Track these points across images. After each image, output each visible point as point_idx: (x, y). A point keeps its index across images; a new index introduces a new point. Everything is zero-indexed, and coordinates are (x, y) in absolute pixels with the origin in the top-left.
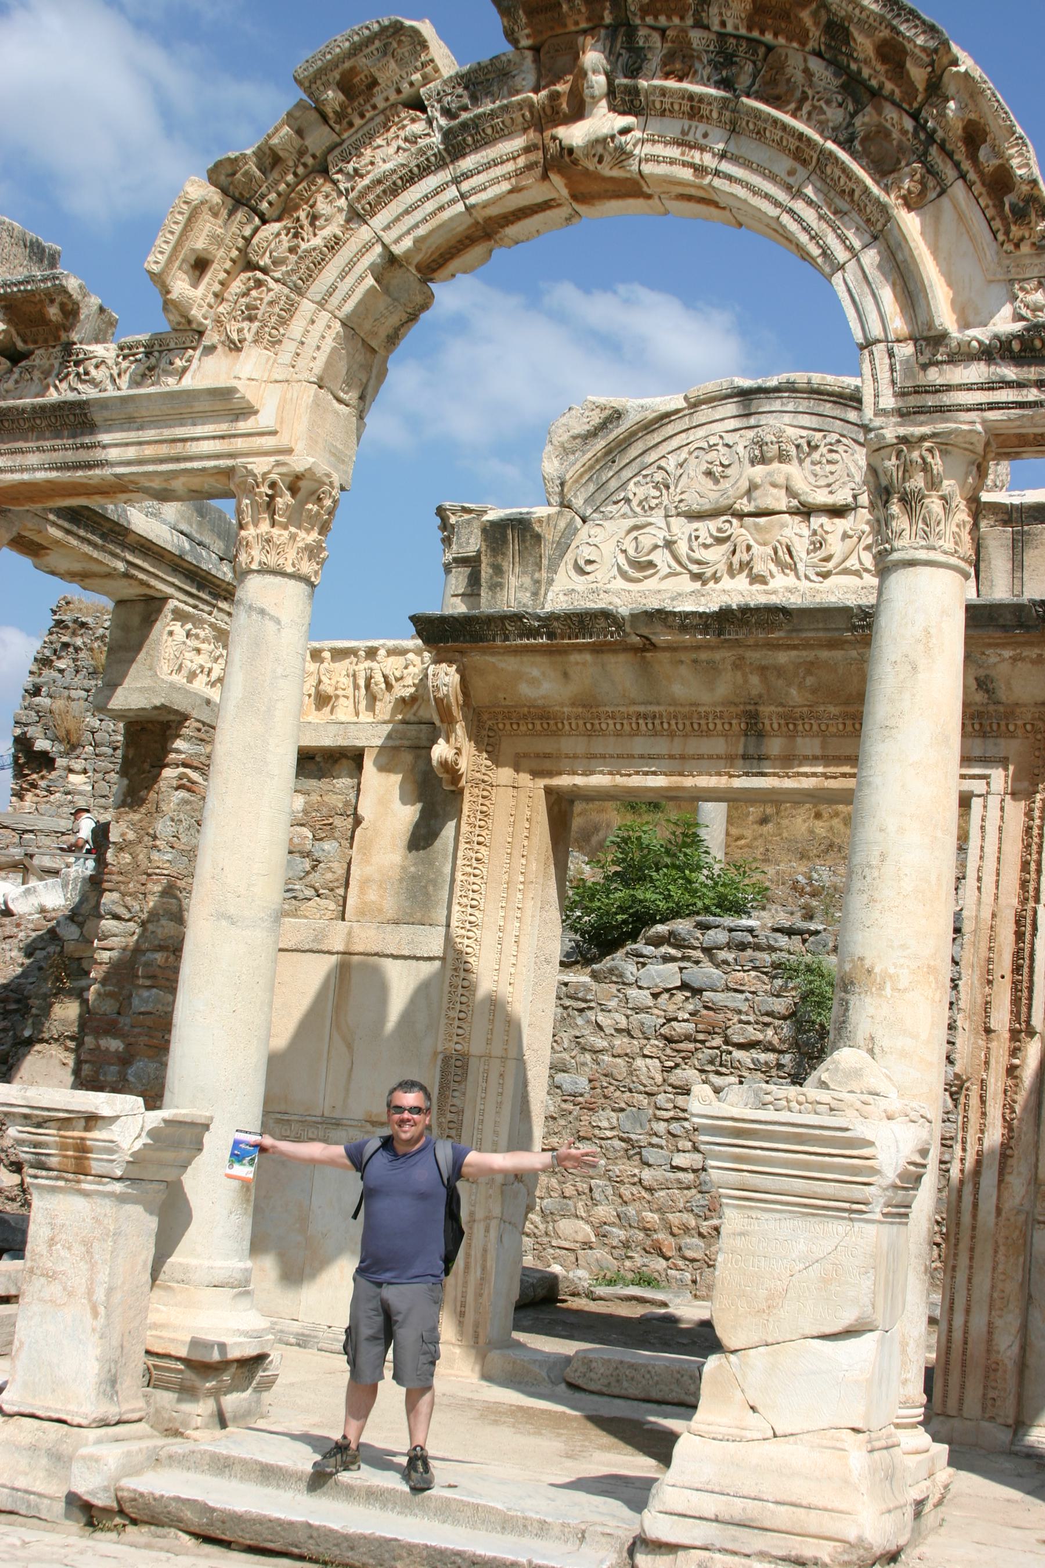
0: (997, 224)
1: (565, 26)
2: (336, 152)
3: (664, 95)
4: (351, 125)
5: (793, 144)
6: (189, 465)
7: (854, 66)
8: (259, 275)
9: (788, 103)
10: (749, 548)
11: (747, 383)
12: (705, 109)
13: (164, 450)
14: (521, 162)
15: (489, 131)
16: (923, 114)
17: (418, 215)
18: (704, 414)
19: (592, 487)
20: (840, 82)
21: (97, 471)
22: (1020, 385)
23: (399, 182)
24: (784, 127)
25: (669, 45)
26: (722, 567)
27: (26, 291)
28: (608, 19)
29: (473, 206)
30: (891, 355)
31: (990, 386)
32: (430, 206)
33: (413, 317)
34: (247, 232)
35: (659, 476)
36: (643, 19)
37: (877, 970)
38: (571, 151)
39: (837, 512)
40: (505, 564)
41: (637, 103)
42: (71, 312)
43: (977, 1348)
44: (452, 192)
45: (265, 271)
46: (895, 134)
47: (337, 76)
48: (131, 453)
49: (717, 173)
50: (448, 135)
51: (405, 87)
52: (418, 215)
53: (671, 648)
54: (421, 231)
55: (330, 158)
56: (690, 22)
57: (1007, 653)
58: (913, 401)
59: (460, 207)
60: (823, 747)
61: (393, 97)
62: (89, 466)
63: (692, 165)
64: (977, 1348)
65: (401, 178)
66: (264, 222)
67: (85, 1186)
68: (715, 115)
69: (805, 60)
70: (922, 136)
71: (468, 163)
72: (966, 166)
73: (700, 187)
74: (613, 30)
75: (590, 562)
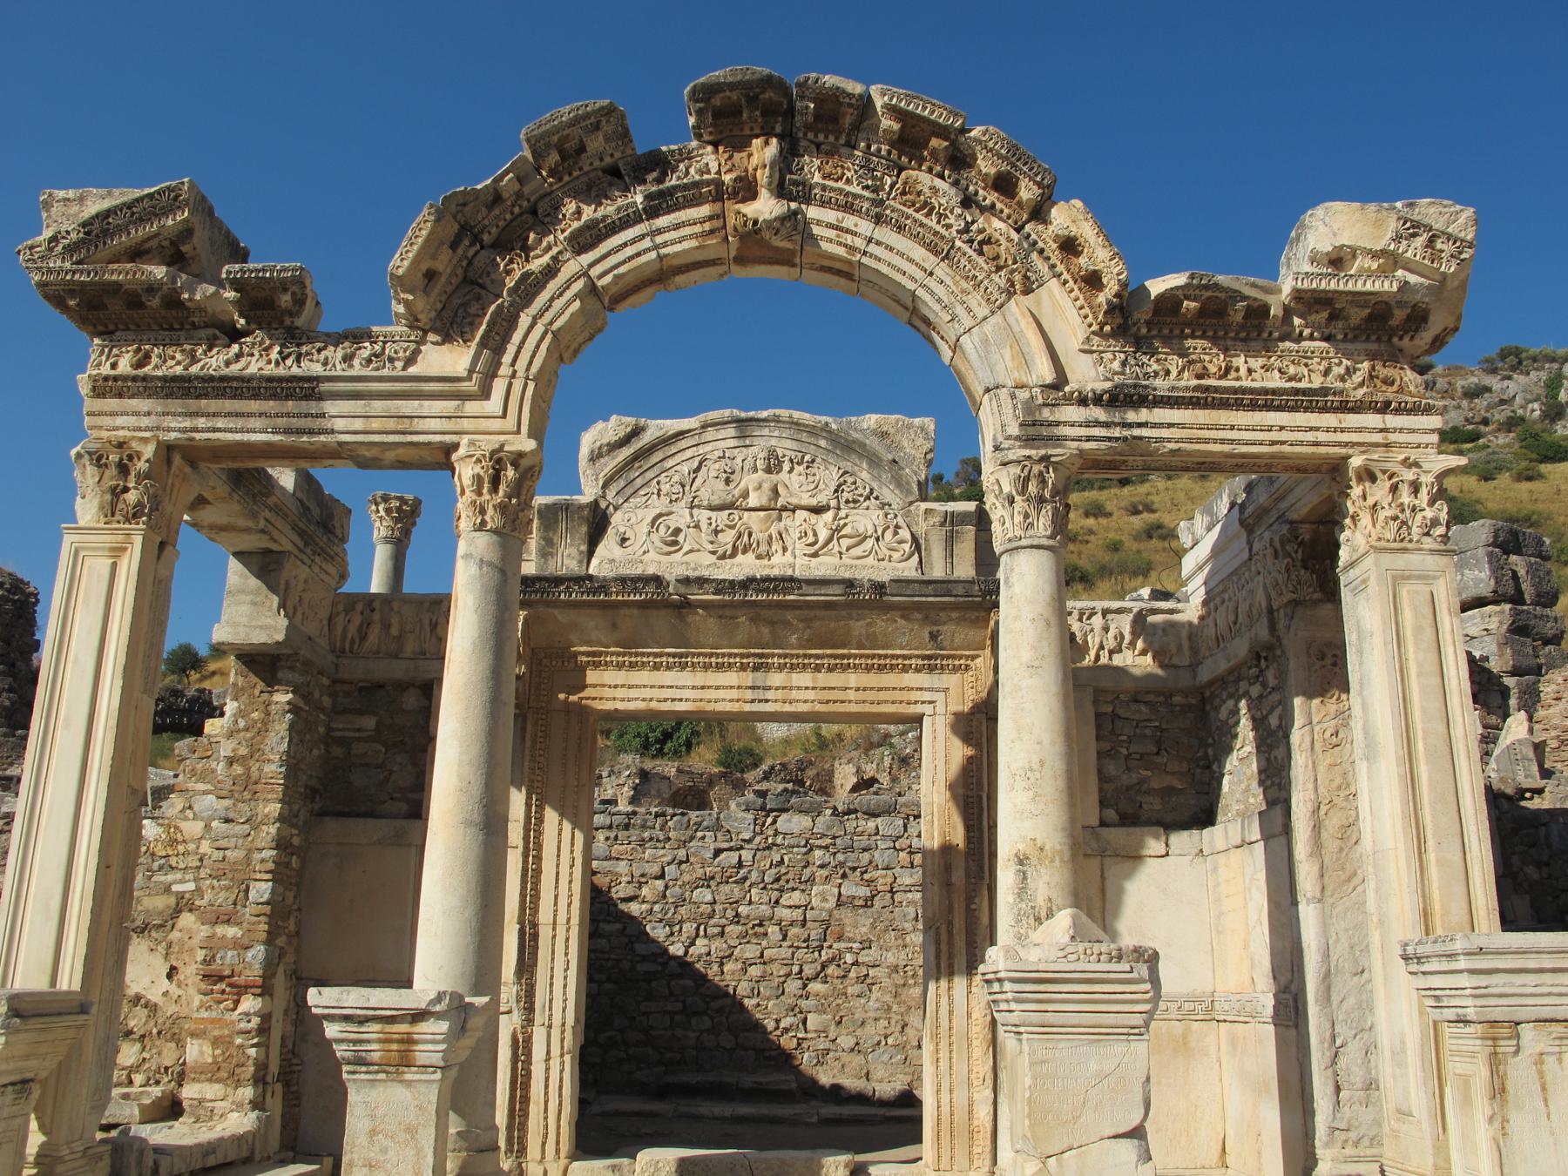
0: (1087, 310)
2: (547, 199)
4: (561, 179)
5: (929, 237)
6: (409, 438)
8: (477, 289)
10: (750, 535)
11: (743, 415)
13: (391, 424)
14: (707, 226)
16: (1028, 228)
17: (620, 257)
18: (710, 434)
19: (622, 483)
21: (322, 438)
22: (1106, 425)
24: (922, 225)
26: (729, 547)
27: (264, 278)
28: (778, 129)
29: (666, 256)
30: (1013, 397)
31: (1087, 424)
32: (629, 251)
33: (591, 338)
34: (472, 252)
35: (676, 478)
37: (1047, 848)
38: (755, 222)
39: (817, 510)
40: (556, 539)
42: (300, 302)
43: (960, 1116)
44: (647, 243)
45: (482, 286)
46: (1003, 240)
47: (555, 138)
48: (358, 424)
49: (865, 253)
50: (646, 197)
52: (620, 257)
53: (705, 605)
54: (622, 270)
55: (540, 204)
56: (842, 141)
57: (955, 615)
58: (1031, 431)
59: (653, 255)
60: (814, 680)
61: (597, 163)
62: (311, 432)
63: (846, 246)
64: (960, 1116)
66: (482, 247)
67: (408, 1077)
70: (1026, 245)
71: (662, 221)
72: (1060, 268)
73: (850, 263)
74: (781, 137)
75: (624, 540)
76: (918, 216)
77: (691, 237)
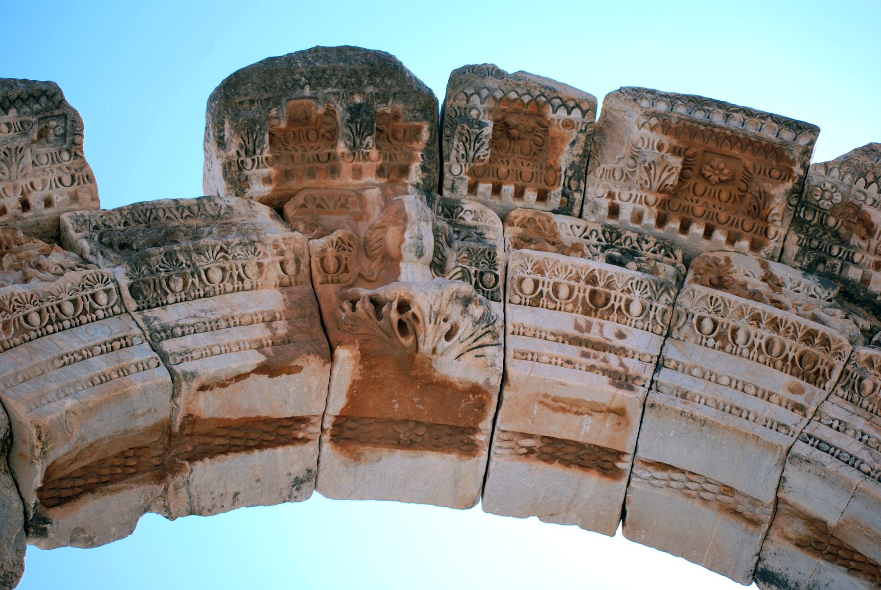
1: (334, 171)
3: (542, 272)
5: (795, 348)
7: (854, 273)
12: (618, 297)
14: (282, 327)
15: (216, 275)
20: (834, 293)
23: (35, 319)
25: (519, 230)
32: (100, 365)
36: (472, 189)
41: (489, 278)
51: (35, 199)
52: (79, 372)
65: (40, 312)
68: (636, 308)
69: (764, 266)
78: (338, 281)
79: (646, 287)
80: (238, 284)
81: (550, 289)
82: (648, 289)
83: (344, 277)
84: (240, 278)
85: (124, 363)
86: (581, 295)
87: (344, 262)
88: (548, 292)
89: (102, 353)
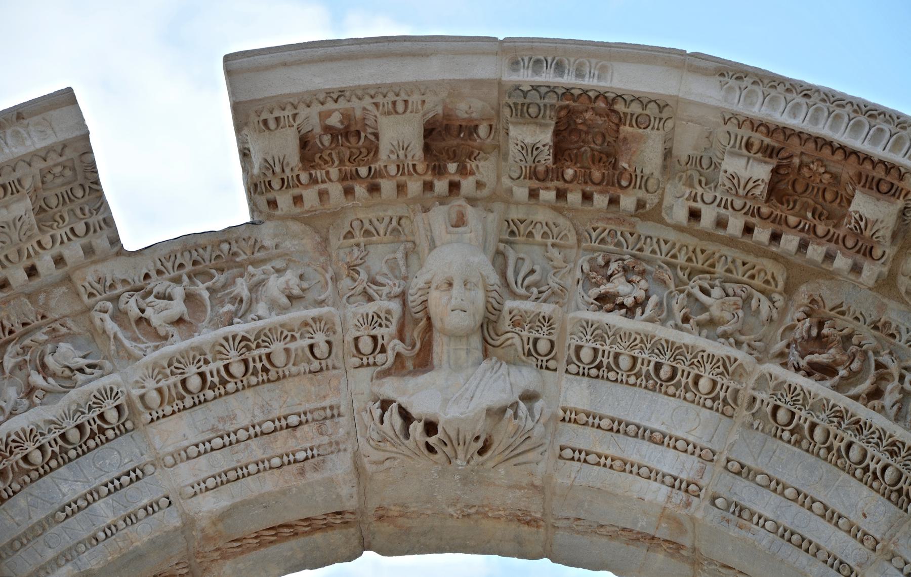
9: (854, 377)
23: (36, 457)
51: (45, 263)
65: (41, 448)
76: (842, 401)
77: (263, 466)
78: (375, 364)
79: (718, 361)
80: (262, 376)
81: (611, 360)
82: (720, 363)
83: (380, 358)
84: (265, 370)
85: (130, 510)
86: (644, 369)
87: (380, 342)
88: (609, 363)
89: (110, 492)
